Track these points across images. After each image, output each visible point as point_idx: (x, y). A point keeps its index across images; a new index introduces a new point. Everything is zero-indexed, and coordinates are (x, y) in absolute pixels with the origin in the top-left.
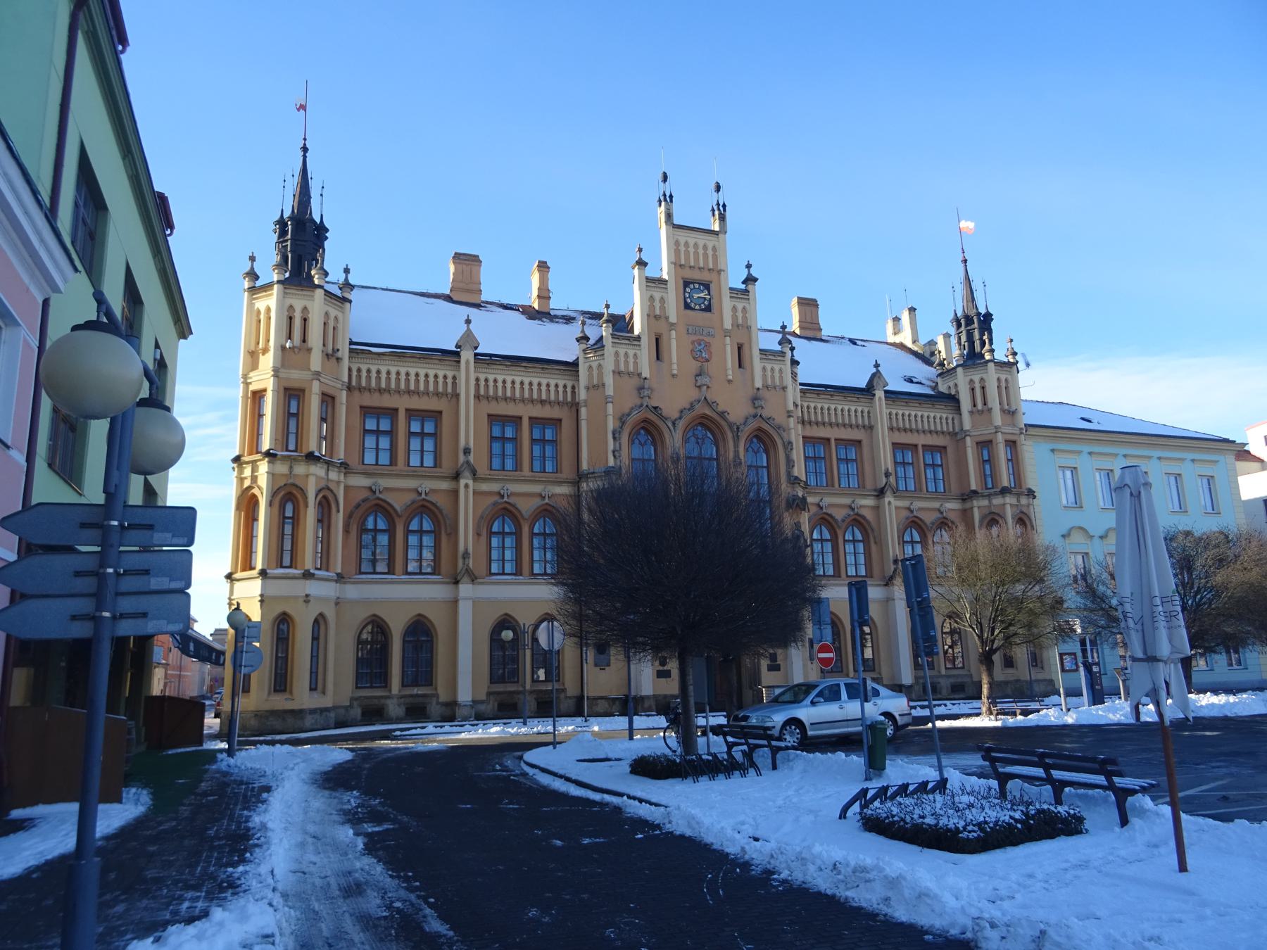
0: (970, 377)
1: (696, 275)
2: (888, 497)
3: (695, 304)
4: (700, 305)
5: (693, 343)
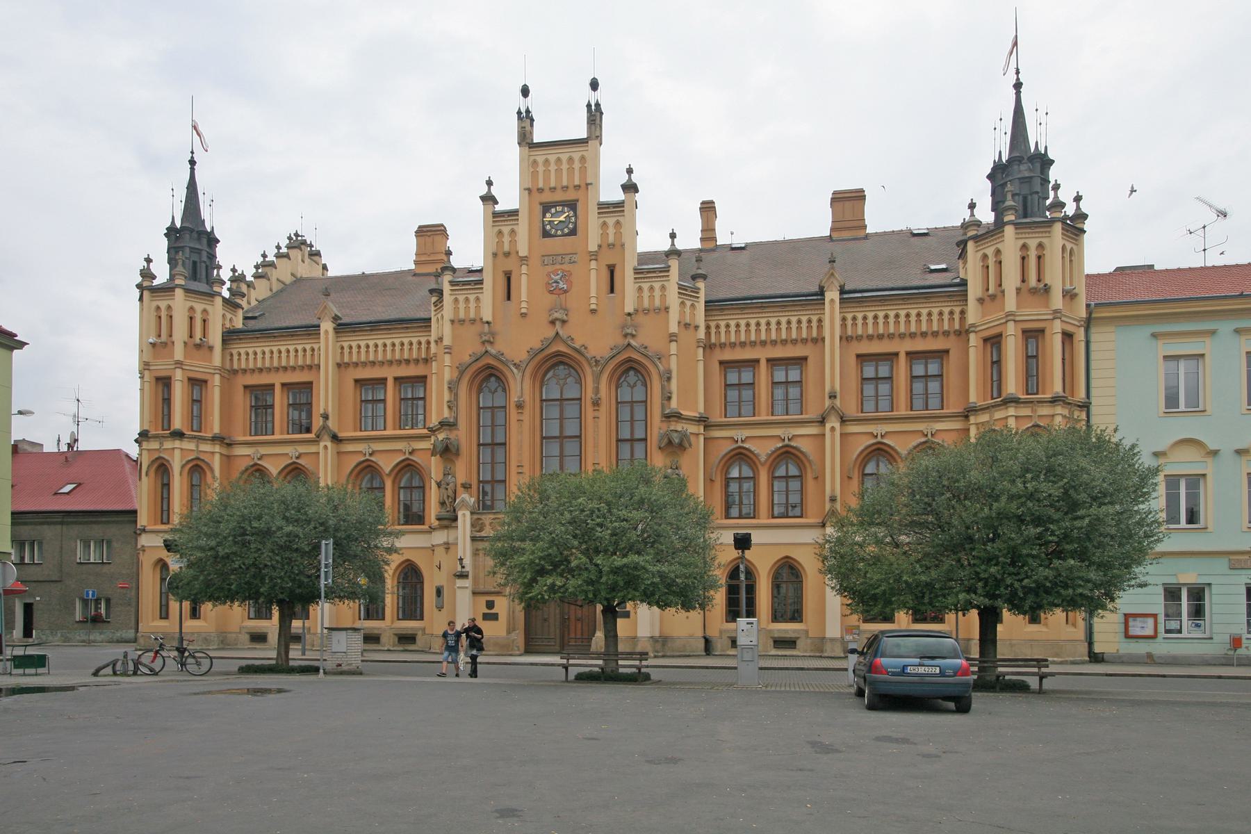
0: (981, 252)
1: (559, 196)
2: (833, 423)
3: (557, 230)
4: (562, 230)
5: (548, 275)
